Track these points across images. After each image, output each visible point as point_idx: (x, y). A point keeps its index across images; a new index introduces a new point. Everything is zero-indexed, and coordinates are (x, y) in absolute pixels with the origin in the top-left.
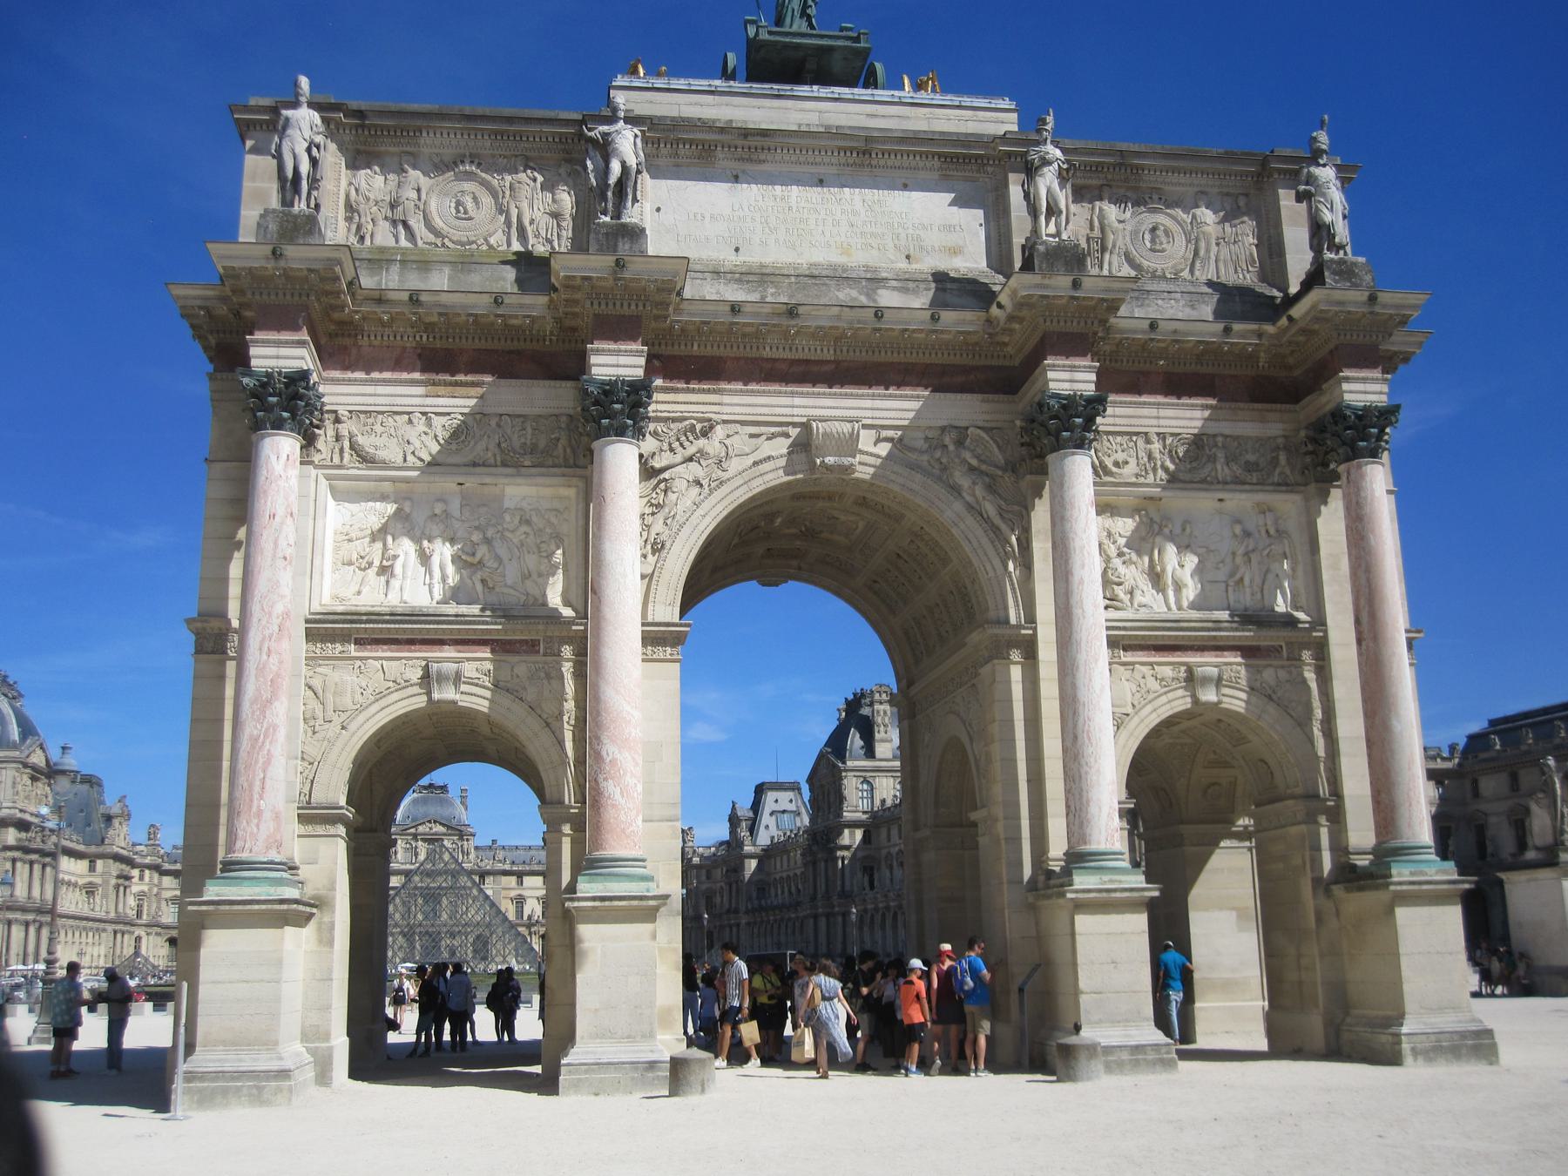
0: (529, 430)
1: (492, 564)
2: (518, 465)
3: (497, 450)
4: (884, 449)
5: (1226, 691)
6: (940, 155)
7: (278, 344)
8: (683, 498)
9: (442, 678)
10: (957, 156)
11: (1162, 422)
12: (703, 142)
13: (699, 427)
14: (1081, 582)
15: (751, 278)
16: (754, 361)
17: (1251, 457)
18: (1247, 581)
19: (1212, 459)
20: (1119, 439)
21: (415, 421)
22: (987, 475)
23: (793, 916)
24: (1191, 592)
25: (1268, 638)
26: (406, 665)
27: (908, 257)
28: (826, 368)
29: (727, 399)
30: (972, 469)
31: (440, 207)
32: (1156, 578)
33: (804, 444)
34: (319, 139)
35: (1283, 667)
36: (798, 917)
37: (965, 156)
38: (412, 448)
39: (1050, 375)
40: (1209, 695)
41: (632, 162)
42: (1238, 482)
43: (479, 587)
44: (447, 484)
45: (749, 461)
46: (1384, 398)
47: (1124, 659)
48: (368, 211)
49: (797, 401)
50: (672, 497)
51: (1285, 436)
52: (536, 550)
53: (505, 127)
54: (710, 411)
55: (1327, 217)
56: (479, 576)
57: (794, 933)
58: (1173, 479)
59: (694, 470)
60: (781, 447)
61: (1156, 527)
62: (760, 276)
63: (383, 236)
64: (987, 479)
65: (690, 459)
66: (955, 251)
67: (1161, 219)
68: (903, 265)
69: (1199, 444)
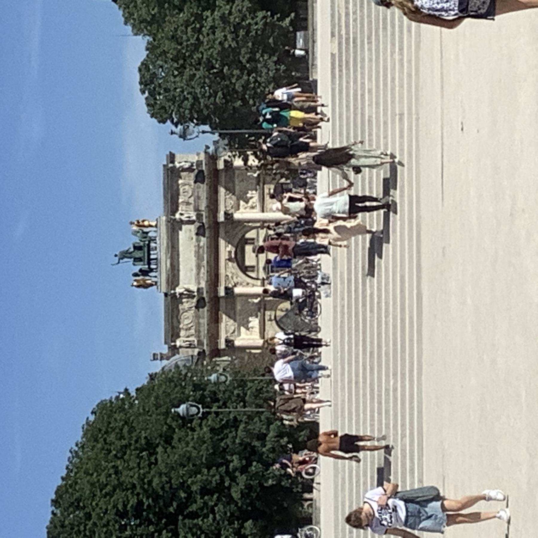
4: (230, 246)
8: (239, 280)
9: (270, 318)
24: (254, 192)
25: (262, 179)
26: (268, 323)
31: (186, 322)
32: (251, 198)
33: (230, 259)
42: (233, 182)
44: (238, 318)
48: (188, 334)
58: (234, 194)
59: (234, 278)
60: (230, 264)
62: (199, 267)
63: (192, 331)
69: (226, 189)
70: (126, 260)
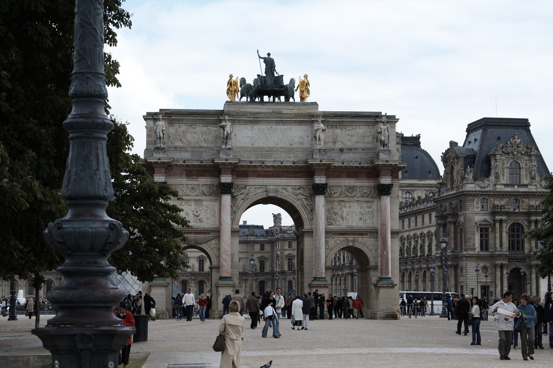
0: (208, 188)
1: (201, 216)
2: (206, 195)
3: (202, 192)
5: (355, 243)
6: (299, 121)
7: (159, 176)
10: (303, 121)
11: (345, 183)
12: (245, 120)
13: (243, 186)
14: (319, 223)
15: (255, 152)
16: (256, 171)
17: (365, 191)
18: (362, 219)
19: (356, 191)
20: (335, 187)
21: (185, 186)
22: (305, 196)
23: (340, 273)
27: (291, 145)
28: (271, 173)
29: (249, 180)
30: (303, 195)
34: (164, 129)
35: (368, 237)
36: (342, 275)
37: (304, 121)
38: (184, 193)
39: (316, 179)
40: (351, 244)
41: (229, 132)
42: (362, 196)
43: (198, 220)
45: (254, 193)
46: (390, 182)
47: (333, 236)
49: (265, 180)
50: (238, 202)
51: (374, 186)
52: (209, 213)
53: (202, 118)
54: (245, 183)
55: (383, 138)
56: (198, 218)
57: (340, 284)
59: (243, 196)
61: (343, 206)
64: (305, 197)
65: (242, 194)
66: (302, 143)
67: (351, 133)
68: (289, 146)
70: (264, 66)
